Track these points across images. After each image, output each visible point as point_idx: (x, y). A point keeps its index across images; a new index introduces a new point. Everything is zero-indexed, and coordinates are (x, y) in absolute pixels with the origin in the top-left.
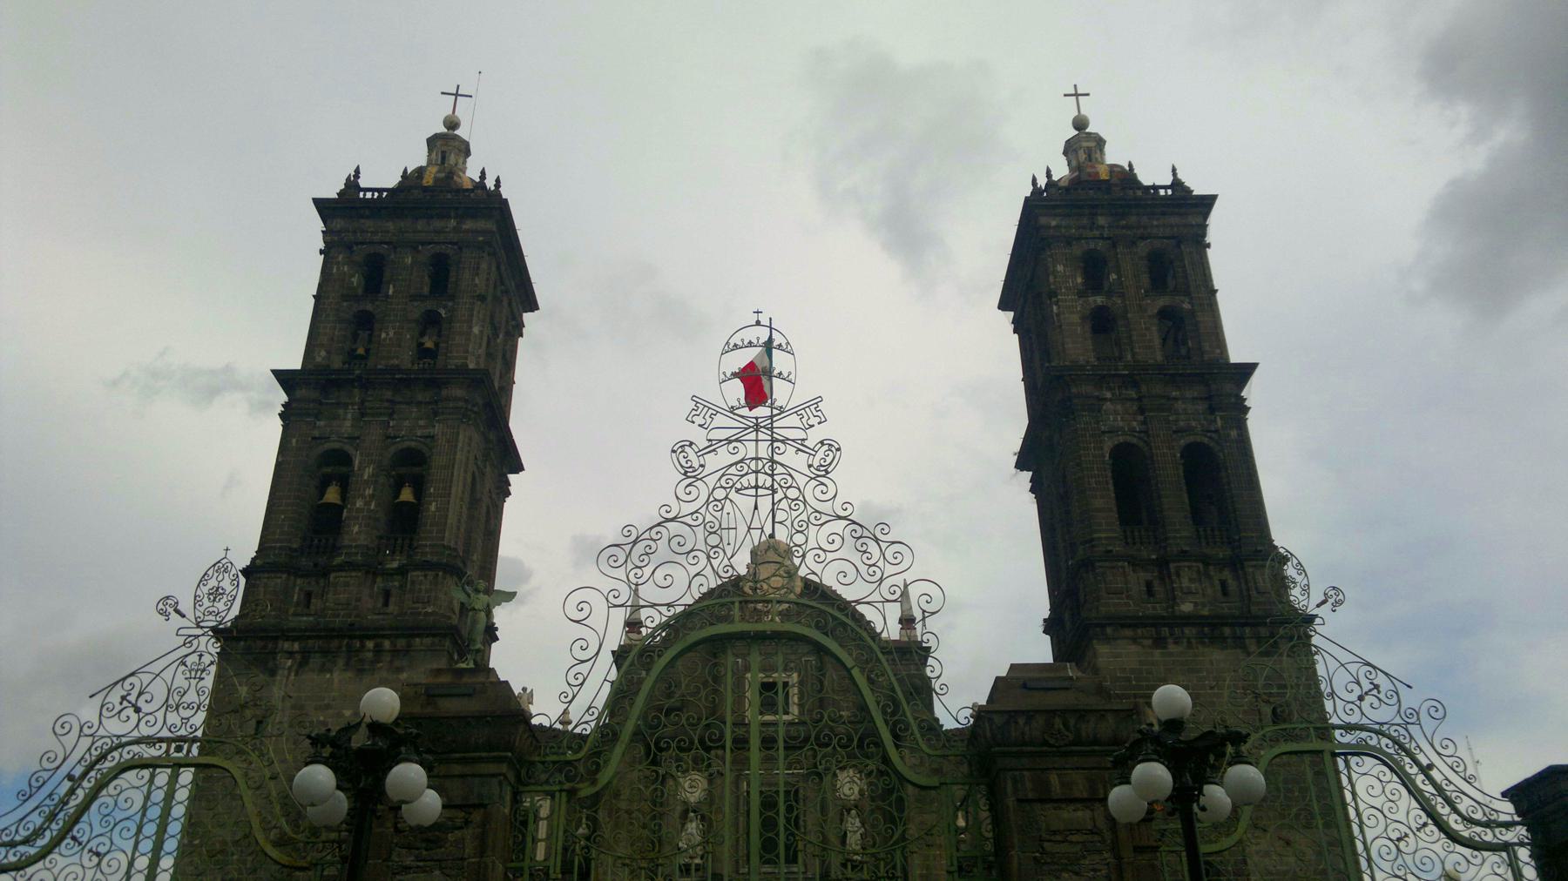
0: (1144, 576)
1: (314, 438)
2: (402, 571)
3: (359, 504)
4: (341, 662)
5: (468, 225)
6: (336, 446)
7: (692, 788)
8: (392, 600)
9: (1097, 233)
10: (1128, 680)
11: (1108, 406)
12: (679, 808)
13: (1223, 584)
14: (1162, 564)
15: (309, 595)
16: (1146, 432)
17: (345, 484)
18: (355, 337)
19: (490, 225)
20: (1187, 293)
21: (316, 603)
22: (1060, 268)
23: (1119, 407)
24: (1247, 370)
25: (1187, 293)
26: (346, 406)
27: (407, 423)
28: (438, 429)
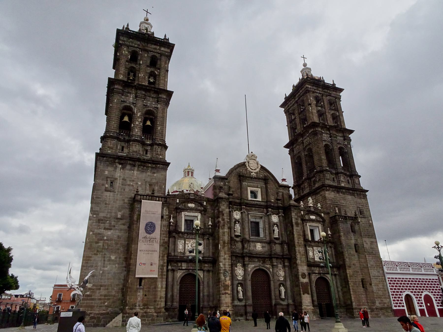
0: (333, 176)
1: (122, 101)
2: (152, 145)
3: (137, 123)
4: (136, 168)
5: (162, 49)
6: (128, 104)
7: (237, 215)
8: (148, 153)
9: (318, 92)
10: (332, 200)
11: (324, 134)
12: (234, 220)
13: (348, 180)
14: (337, 174)
15: (123, 148)
16: (332, 142)
17: (131, 118)
18: (129, 74)
19: (169, 51)
20: (338, 111)
21: (126, 150)
22: (311, 98)
23: (326, 135)
24: (351, 132)
25: (338, 111)
26: (130, 93)
27: (149, 102)
28: (159, 106)
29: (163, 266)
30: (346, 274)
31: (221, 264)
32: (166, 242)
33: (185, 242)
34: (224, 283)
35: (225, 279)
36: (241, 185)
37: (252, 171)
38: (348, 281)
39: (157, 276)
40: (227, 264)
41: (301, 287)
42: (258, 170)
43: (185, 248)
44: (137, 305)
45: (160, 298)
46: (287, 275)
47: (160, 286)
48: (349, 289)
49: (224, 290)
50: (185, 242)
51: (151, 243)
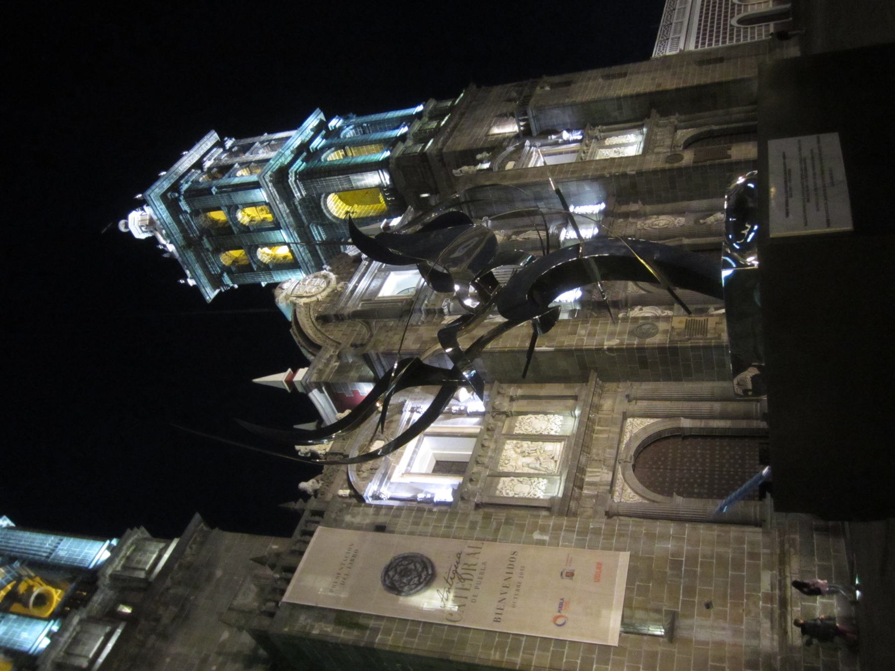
29: (583, 532)
30: (678, 90)
31: (607, 344)
32: (487, 517)
33: (507, 475)
34: (679, 334)
35: (666, 332)
36: (356, 315)
37: (329, 290)
38: (698, 87)
39: (624, 558)
40: (610, 328)
41: (708, 163)
42: (333, 276)
43: (530, 476)
44: (754, 642)
45: (726, 544)
46: (669, 206)
47: (670, 546)
48: (720, 84)
49: (703, 330)
50: (507, 475)
51: (476, 574)
